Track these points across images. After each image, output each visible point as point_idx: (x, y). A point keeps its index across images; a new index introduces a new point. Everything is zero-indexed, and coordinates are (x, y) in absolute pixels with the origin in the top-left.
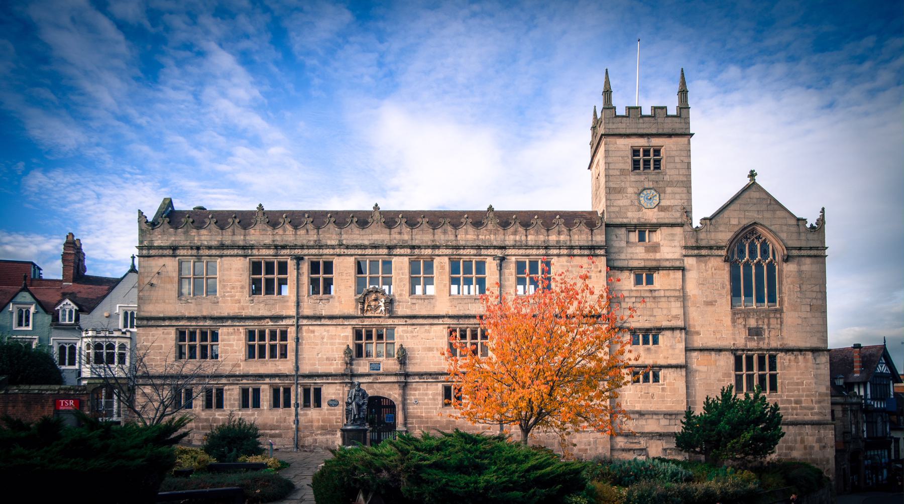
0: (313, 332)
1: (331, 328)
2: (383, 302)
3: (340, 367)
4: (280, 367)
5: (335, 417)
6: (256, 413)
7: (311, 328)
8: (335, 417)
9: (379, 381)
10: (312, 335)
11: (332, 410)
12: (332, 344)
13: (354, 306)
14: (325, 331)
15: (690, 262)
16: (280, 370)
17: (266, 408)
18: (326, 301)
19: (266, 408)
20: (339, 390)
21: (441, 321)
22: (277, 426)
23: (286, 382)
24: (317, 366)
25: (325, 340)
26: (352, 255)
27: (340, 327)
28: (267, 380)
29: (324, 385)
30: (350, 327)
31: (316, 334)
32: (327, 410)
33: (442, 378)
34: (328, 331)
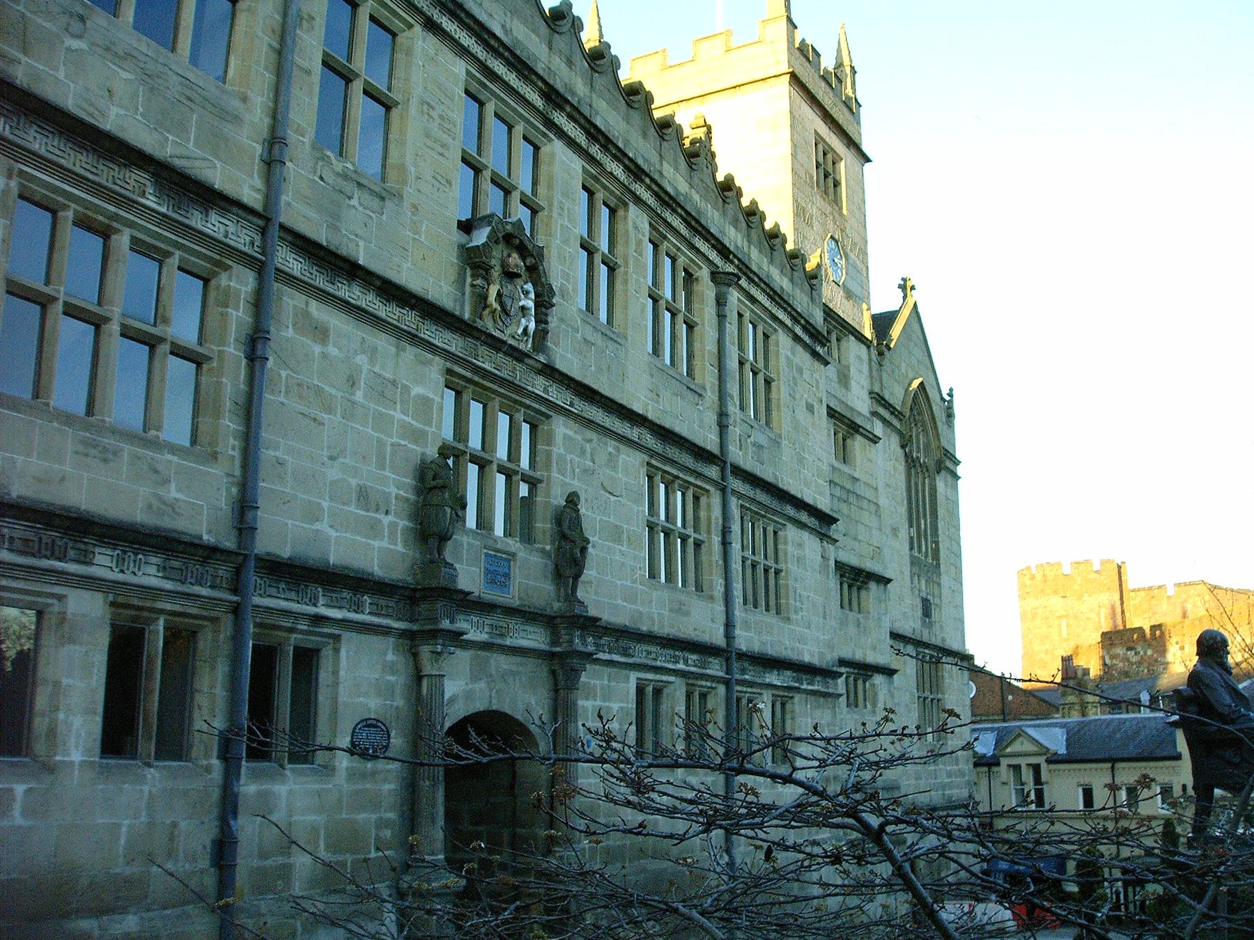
0: (321, 333)
1: (382, 341)
2: (532, 296)
3: (400, 548)
4: (173, 493)
5: (374, 817)
6: (20, 789)
7: (316, 309)
8: (374, 817)
9: (508, 642)
10: (317, 349)
11: (363, 776)
12: (381, 422)
13: (452, 274)
14: (364, 352)
15: (878, 429)
16: (172, 506)
17: (76, 756)
18: (376, 203)
19: (76, 756)
20: (392, 669)
21: (634, 433)
22: (128, 881)
23: (205, 592)
24: (323, 526)
25: (359, 396)
26: (464, 52)
27: (411, 352)
28: (104, 564)
29: (346, 635)
30: (438, 363)
31: (333, 350)
32: (352, 775)
33: (641, 654)
34: (373, 353)
